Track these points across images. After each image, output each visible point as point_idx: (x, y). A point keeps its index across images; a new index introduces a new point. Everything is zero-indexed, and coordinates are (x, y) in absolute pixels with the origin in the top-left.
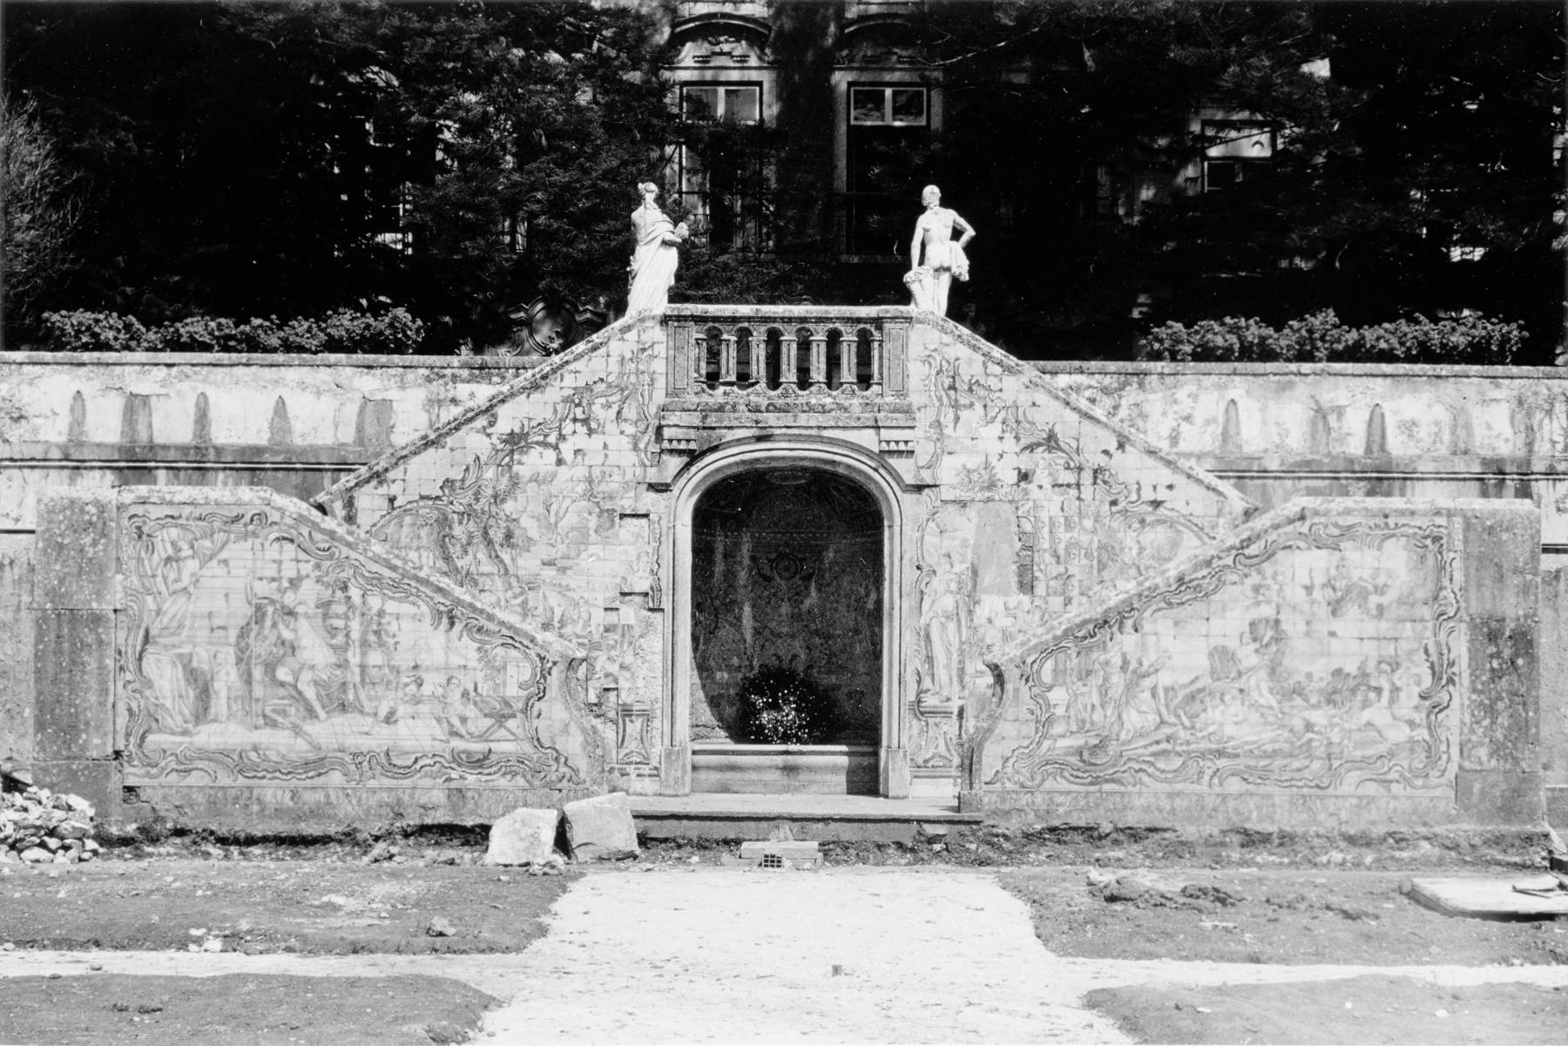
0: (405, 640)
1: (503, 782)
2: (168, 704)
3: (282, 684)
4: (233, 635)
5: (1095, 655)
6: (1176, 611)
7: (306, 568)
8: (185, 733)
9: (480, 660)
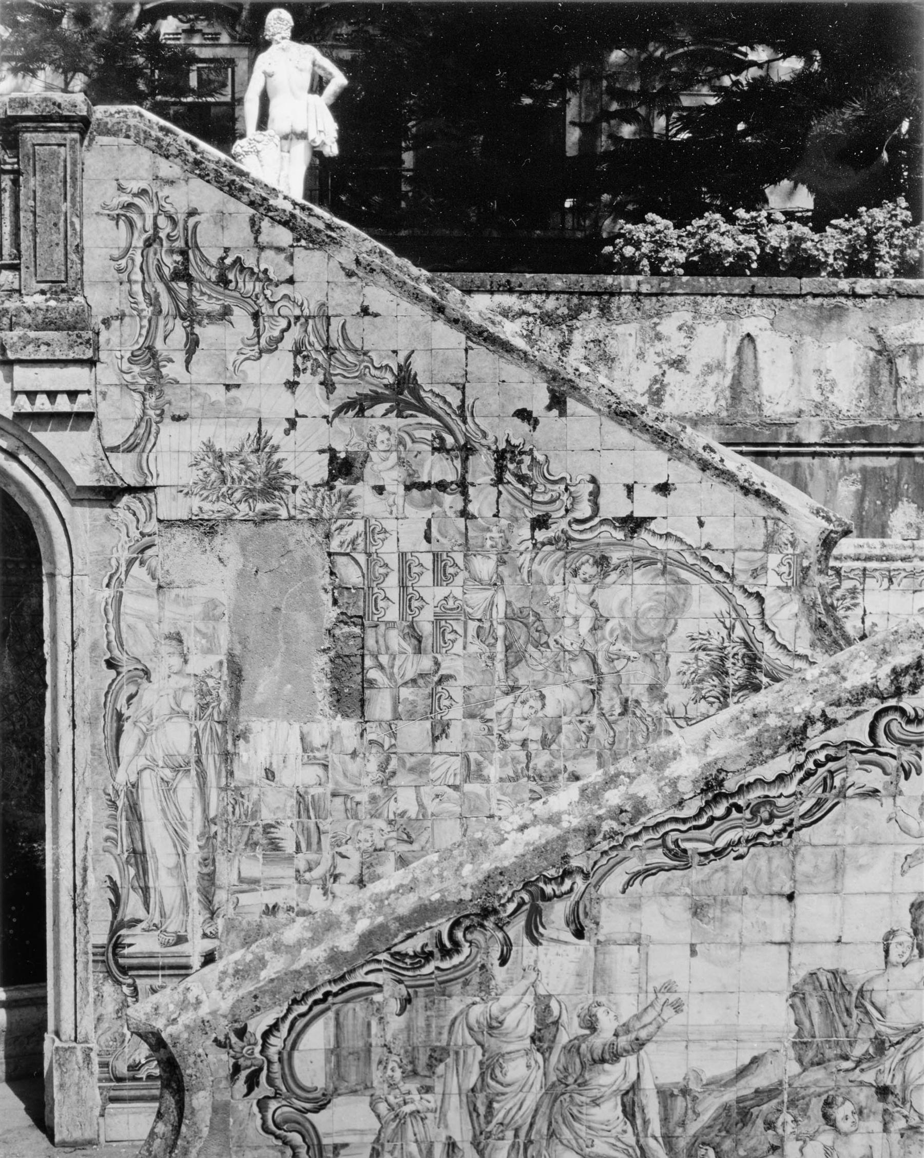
5: (456, 1005)
6: (696, 874)
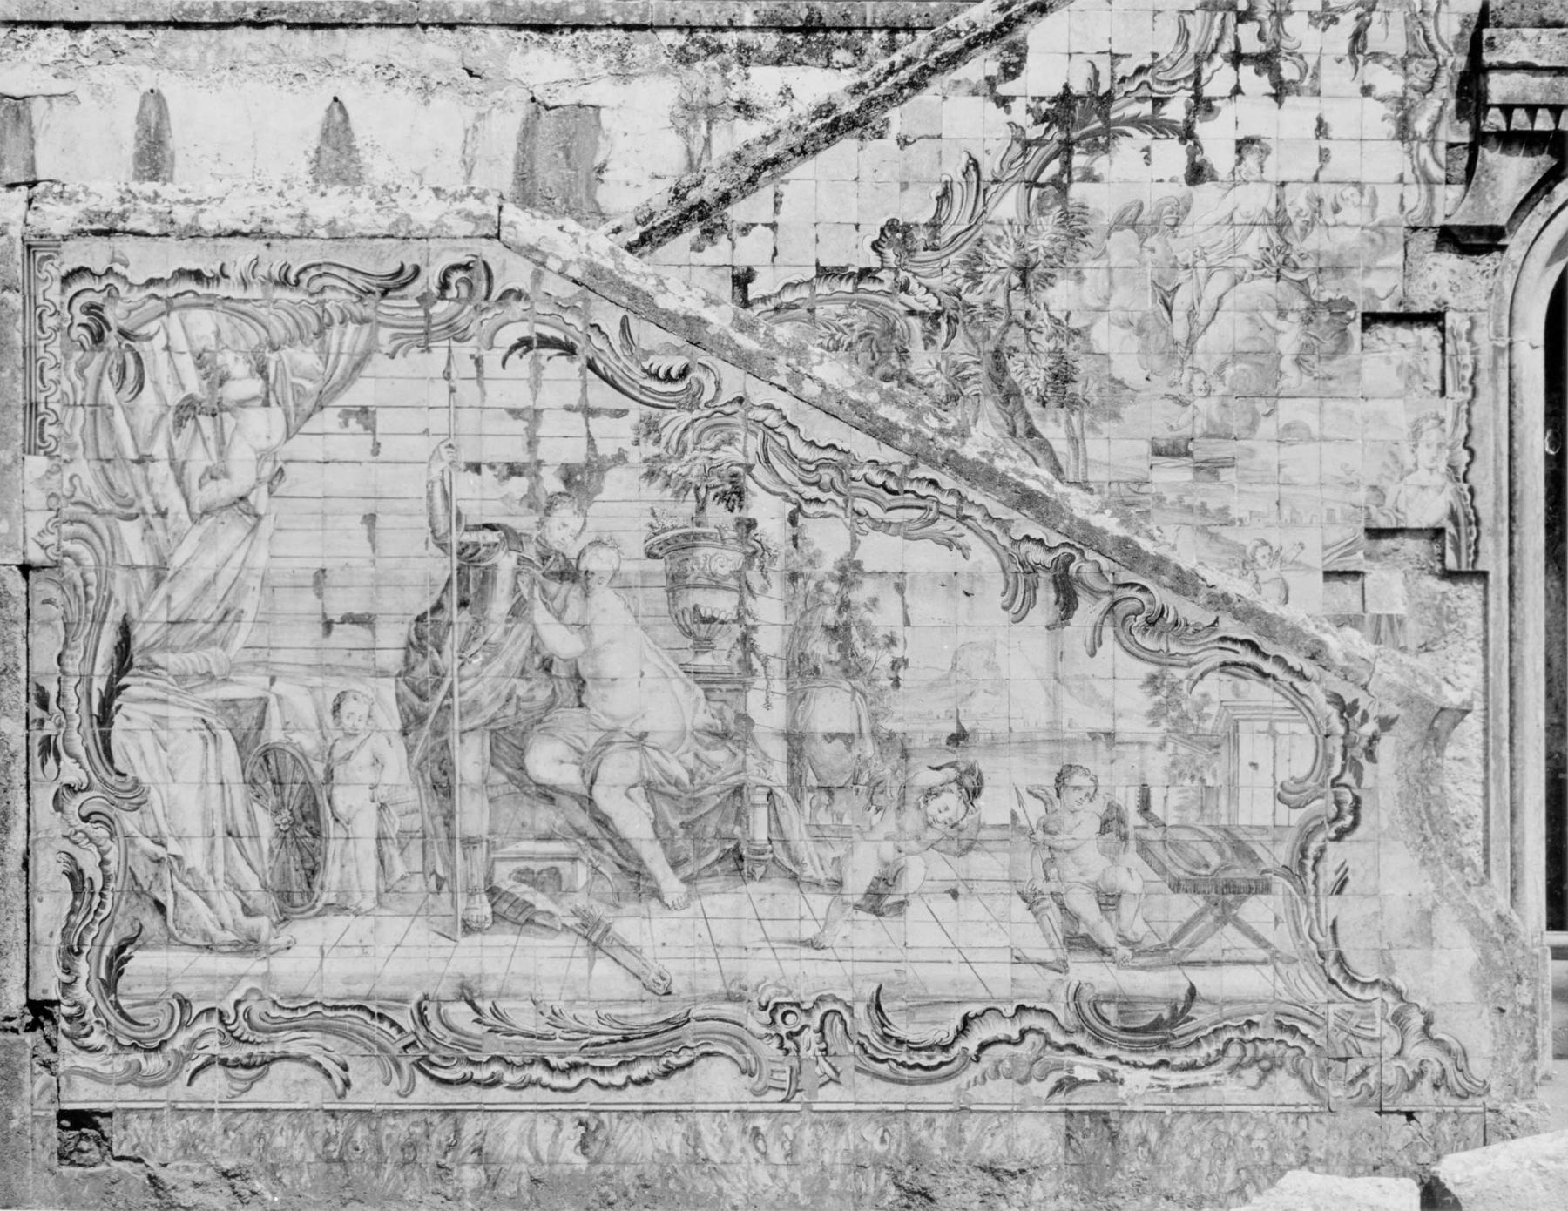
0: (927, 653)
1: (1234, 1091)
2: (195, 856)
3: (548, 794)
4: (392, 637)
7: (615, 434)
8: (249, 946)
9: (1155, 715)
